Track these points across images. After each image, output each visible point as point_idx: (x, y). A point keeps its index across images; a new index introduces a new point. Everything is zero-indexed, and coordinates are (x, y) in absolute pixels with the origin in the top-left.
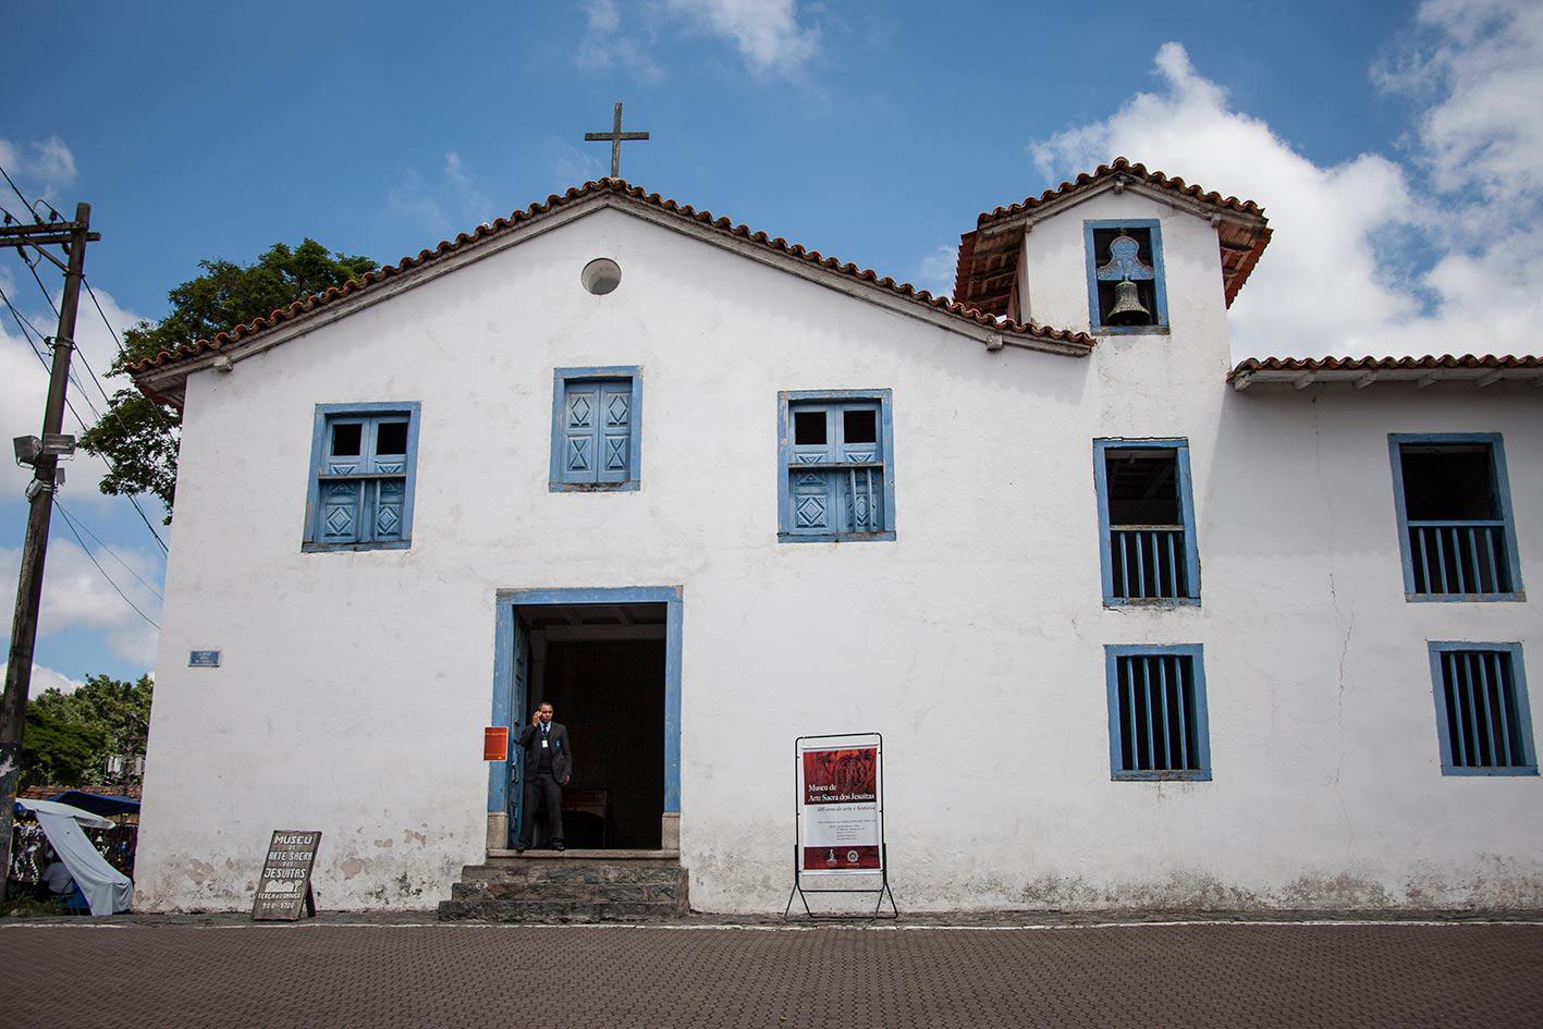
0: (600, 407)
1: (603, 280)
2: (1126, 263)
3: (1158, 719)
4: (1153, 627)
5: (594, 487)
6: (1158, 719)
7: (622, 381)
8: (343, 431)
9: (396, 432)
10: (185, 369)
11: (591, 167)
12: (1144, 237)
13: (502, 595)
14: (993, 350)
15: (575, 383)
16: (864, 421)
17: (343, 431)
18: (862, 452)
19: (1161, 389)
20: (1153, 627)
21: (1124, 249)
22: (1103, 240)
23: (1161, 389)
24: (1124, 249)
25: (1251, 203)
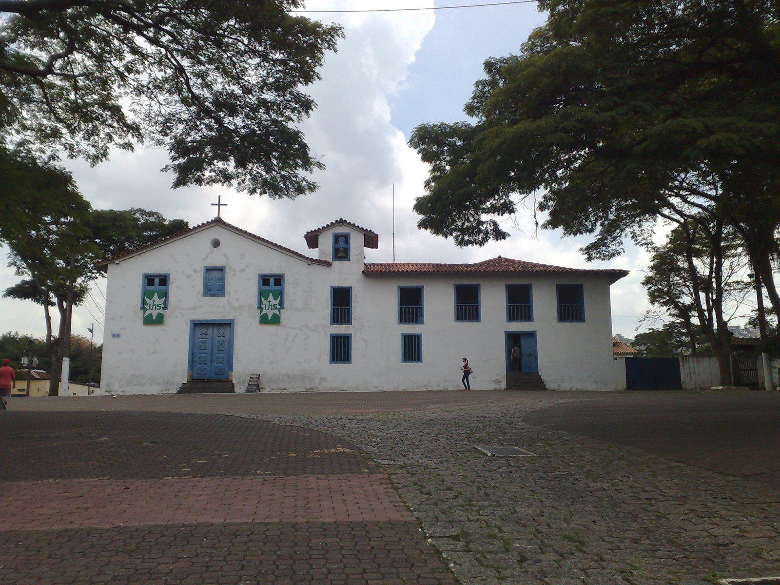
0: (215, 274)
1: (216, 244)
2: (342, 244)
3: (341, 349)
4: (341, 329)
5: (213, 295)
6: (341, 349)
7: (221, 270)
8: (149, 280)
9: (164, 280)
10: (107, 263)
11: (212, 216)
12: (346, 238)
13: (191, 321)
14: (309, 264)
15: (208, 270)
16: (279, 280)
17: (149, 280)
18: (278, 288)
19: (346, 274)
20: (341, 329)
21: (342, 240)
22: (337, 238)
23: (346, 274)
24: (342, 240)
25: (371, 230)
